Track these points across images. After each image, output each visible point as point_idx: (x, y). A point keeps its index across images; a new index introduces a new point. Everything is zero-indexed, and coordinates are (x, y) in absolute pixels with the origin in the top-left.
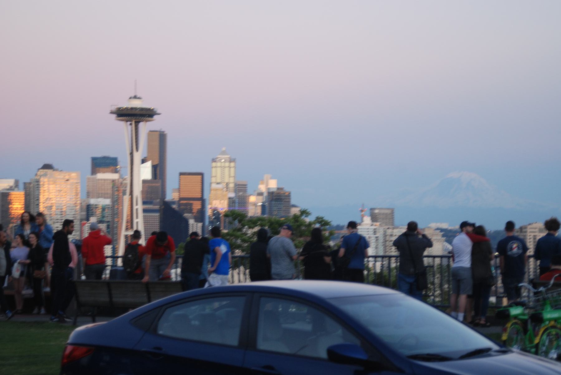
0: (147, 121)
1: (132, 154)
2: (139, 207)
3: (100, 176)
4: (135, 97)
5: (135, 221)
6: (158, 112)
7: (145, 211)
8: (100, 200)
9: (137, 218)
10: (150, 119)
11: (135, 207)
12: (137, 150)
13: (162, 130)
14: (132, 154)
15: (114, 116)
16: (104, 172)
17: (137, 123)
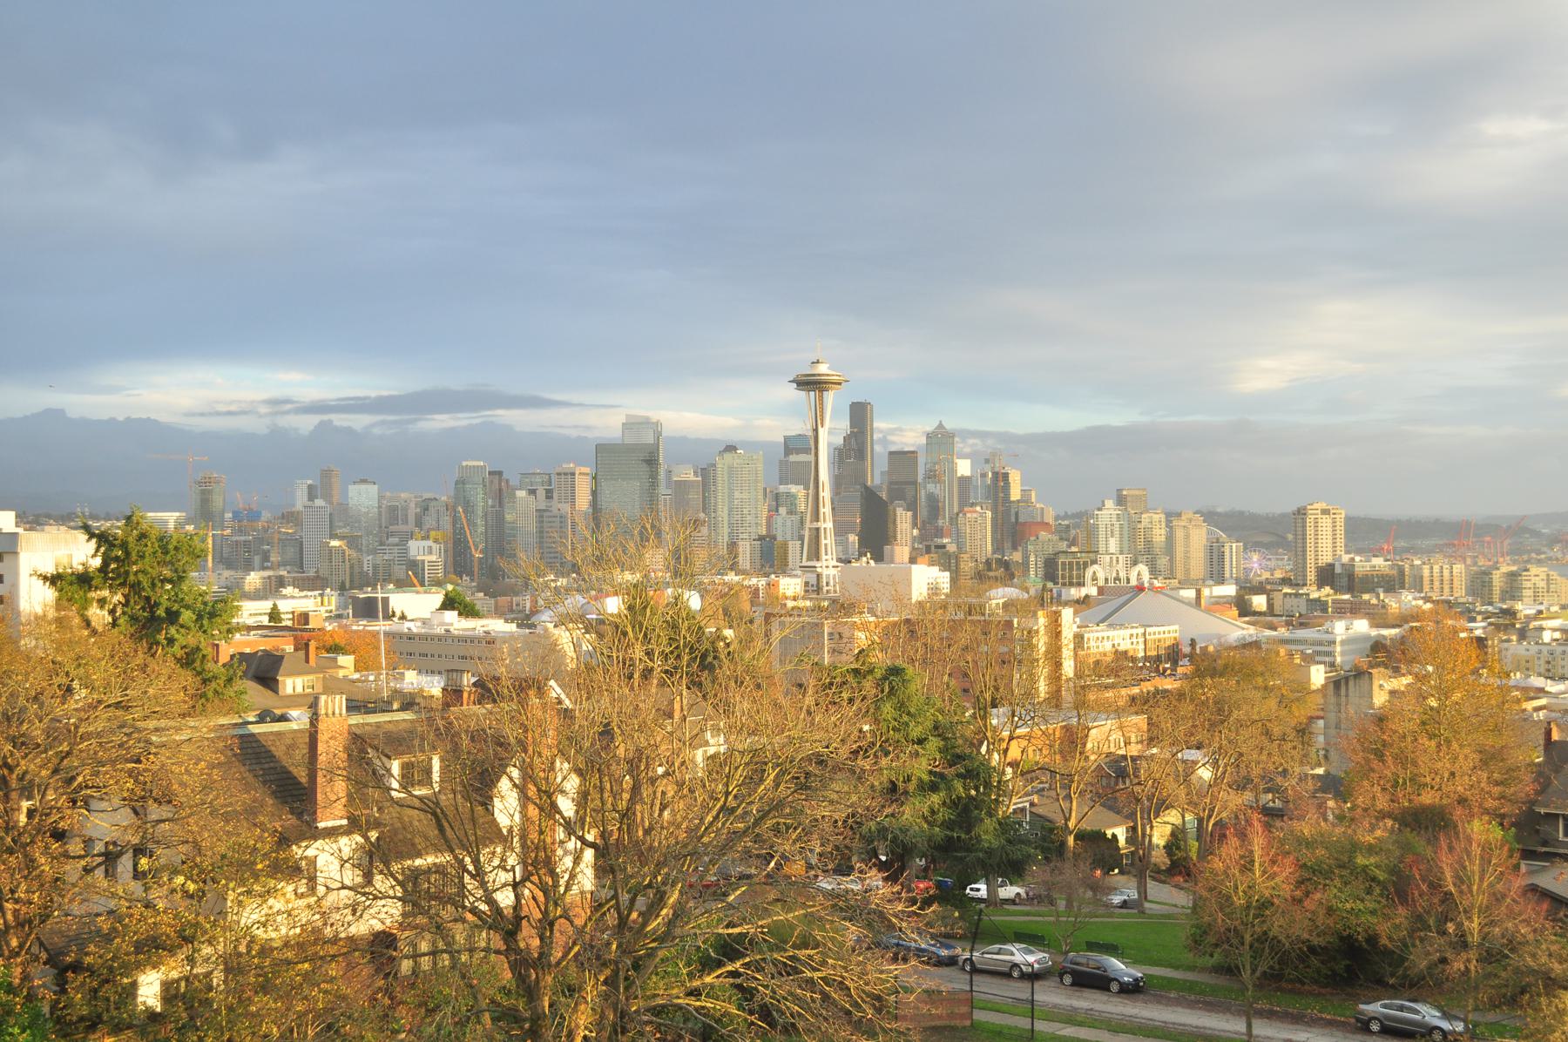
3: (793, 458)
5: (822, 510)
14: (816, 430)
17: (822, 391)
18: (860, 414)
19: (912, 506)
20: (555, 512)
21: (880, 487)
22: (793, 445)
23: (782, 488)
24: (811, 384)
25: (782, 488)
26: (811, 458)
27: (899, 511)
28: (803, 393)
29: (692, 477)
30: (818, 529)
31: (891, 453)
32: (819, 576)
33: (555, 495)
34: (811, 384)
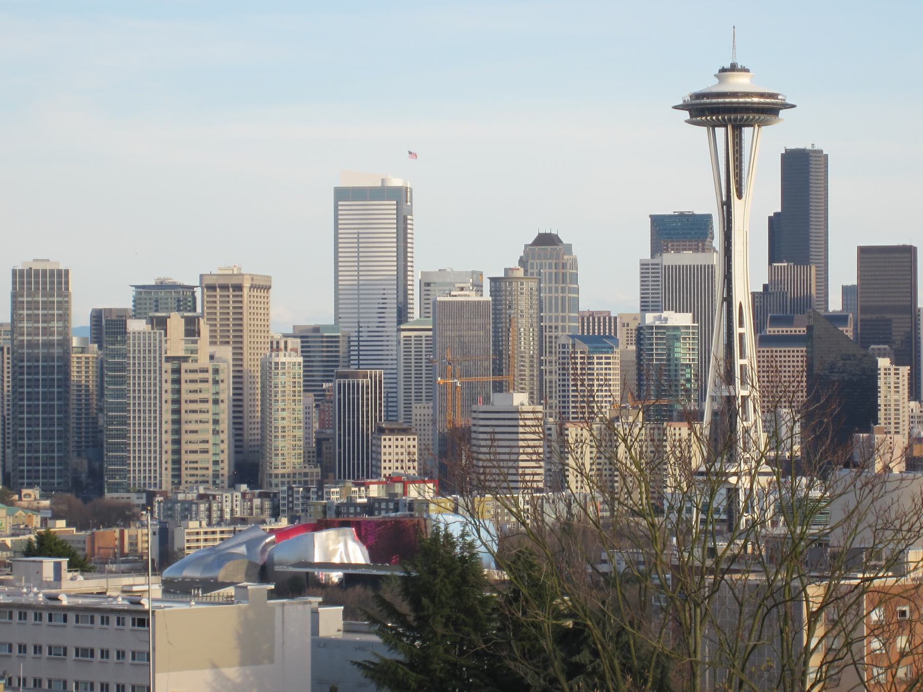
0: (762, 124)
1: (727, 206)
2: (746, 330)
3: (671, 259)
4: (733, 68)
6: (788, 101)
7: (763, 340)
8: (665, 314)
9: (741, 357)
10: (768, 117)
11: (737, 330)
12: (740, 196)
13: (816, 148)
14: (727, 206)
15: (686, 115)
16: (678, 251)
17: (738, 128)
18: (802, 173)
19: (905, 354)
20: (203, 361)
21: (840, 319)
22: (676, 231)
23: (650, 318)
24: (724, 113)
25: (650, 318)
26: (716, 260)
27: (884, 363)
28: (702, 132)
29: (473, 297)
30: (730, 400)
31: (864, 252)
32: (733, 492)
33: (204, 329)
34: (724, 113)
